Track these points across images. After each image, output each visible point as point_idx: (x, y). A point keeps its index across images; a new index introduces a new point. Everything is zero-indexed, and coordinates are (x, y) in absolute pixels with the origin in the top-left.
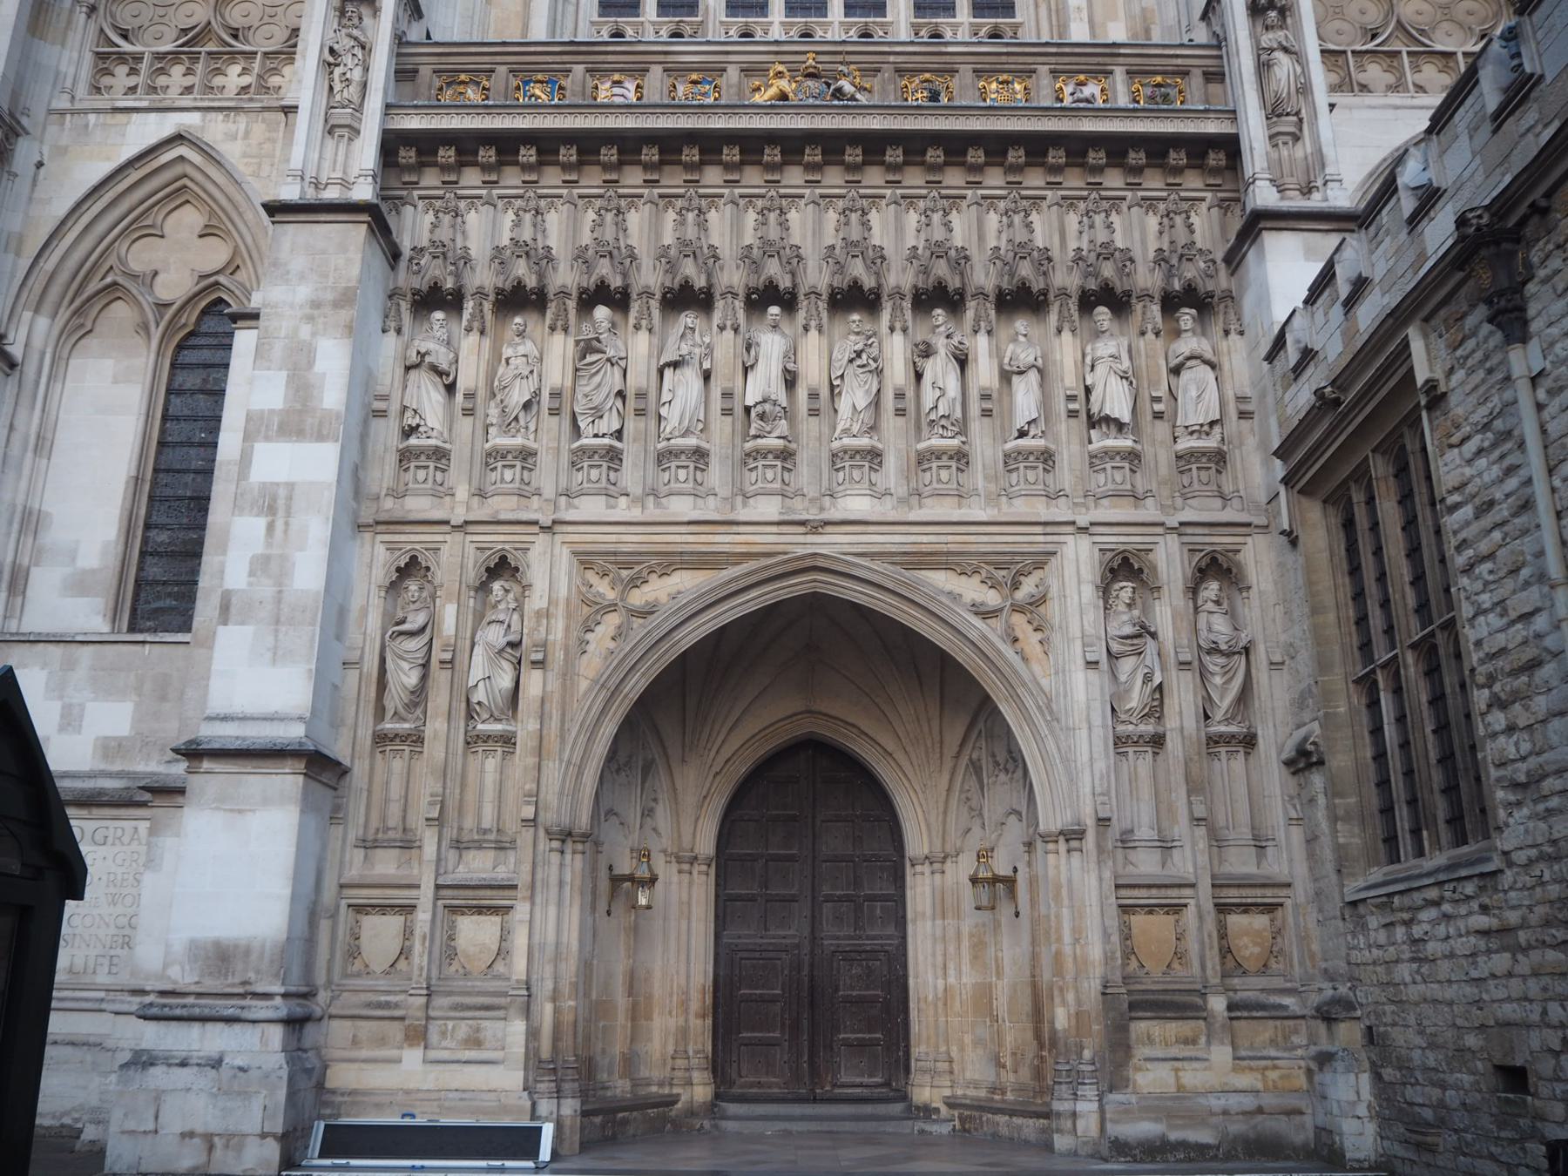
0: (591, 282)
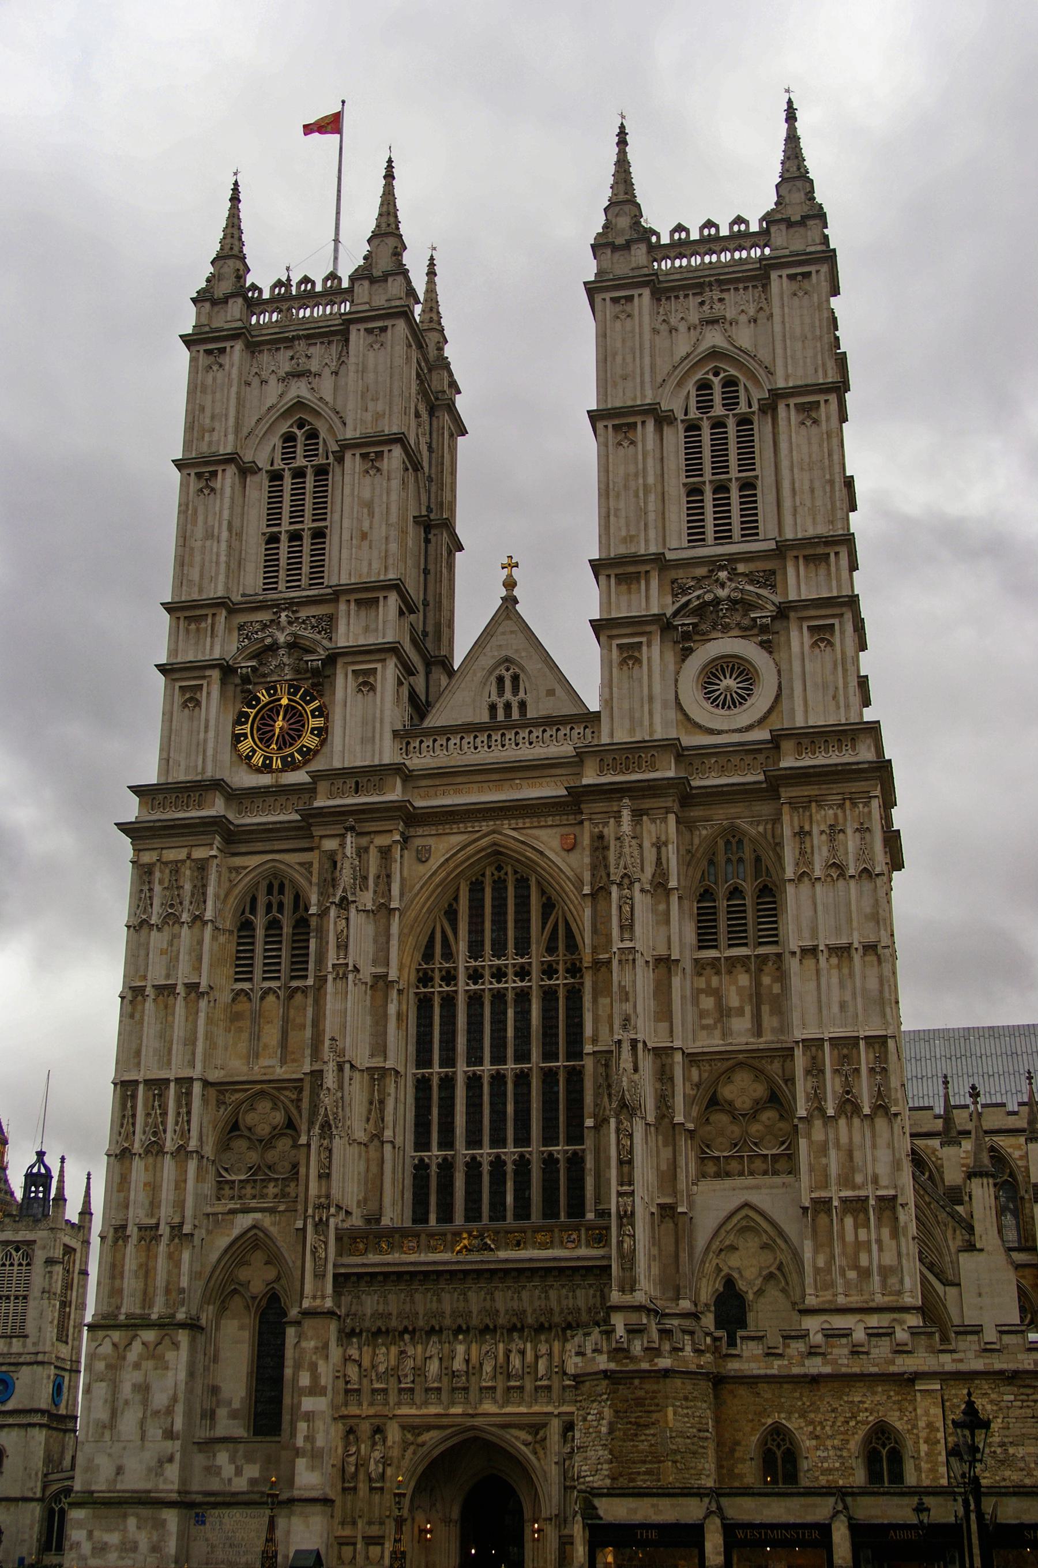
0: (401, 1328)
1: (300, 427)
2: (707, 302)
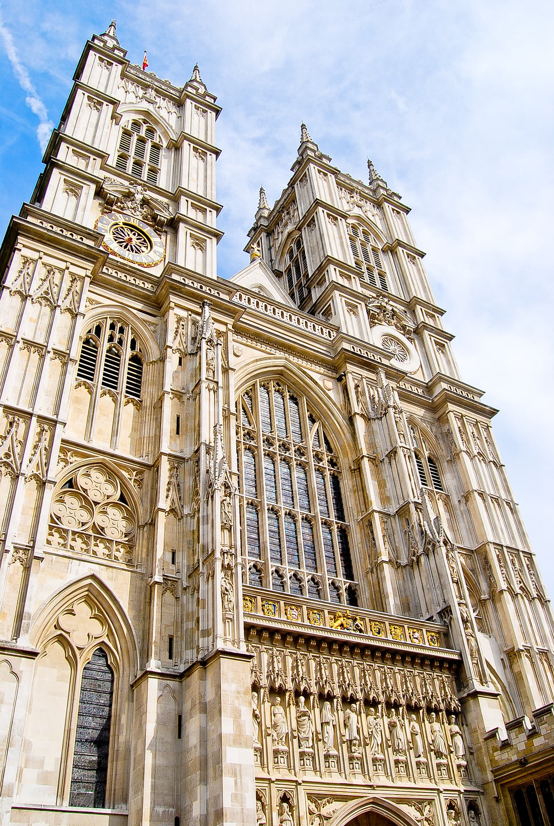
1: (145, 123)
2: (355, 198)
